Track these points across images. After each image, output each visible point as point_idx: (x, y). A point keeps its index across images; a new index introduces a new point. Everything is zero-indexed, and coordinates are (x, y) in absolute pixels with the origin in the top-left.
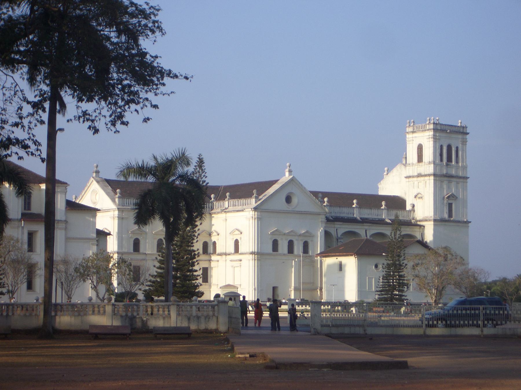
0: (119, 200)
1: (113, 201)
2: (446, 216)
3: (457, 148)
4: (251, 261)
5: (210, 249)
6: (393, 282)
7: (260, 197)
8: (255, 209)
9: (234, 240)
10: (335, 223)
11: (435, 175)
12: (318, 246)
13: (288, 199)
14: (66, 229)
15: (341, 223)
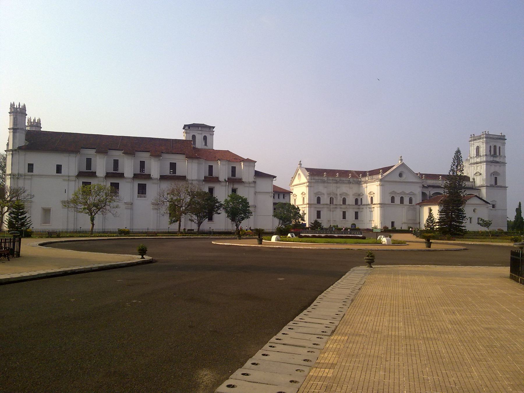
0: (309, 177)
1: (306, 178)
2: (493, 183)
3: (500, 147)
4: (379, 208)
5: (359, 203)
6: (452, 215)
7: (384, 175)
8: (381, 180)
9: (371, 197)
10: (429, 188)
11: (487, 162)
12: (418, 199)
13: (400, 175)
14: (254, 187)
15: (432, 188)
